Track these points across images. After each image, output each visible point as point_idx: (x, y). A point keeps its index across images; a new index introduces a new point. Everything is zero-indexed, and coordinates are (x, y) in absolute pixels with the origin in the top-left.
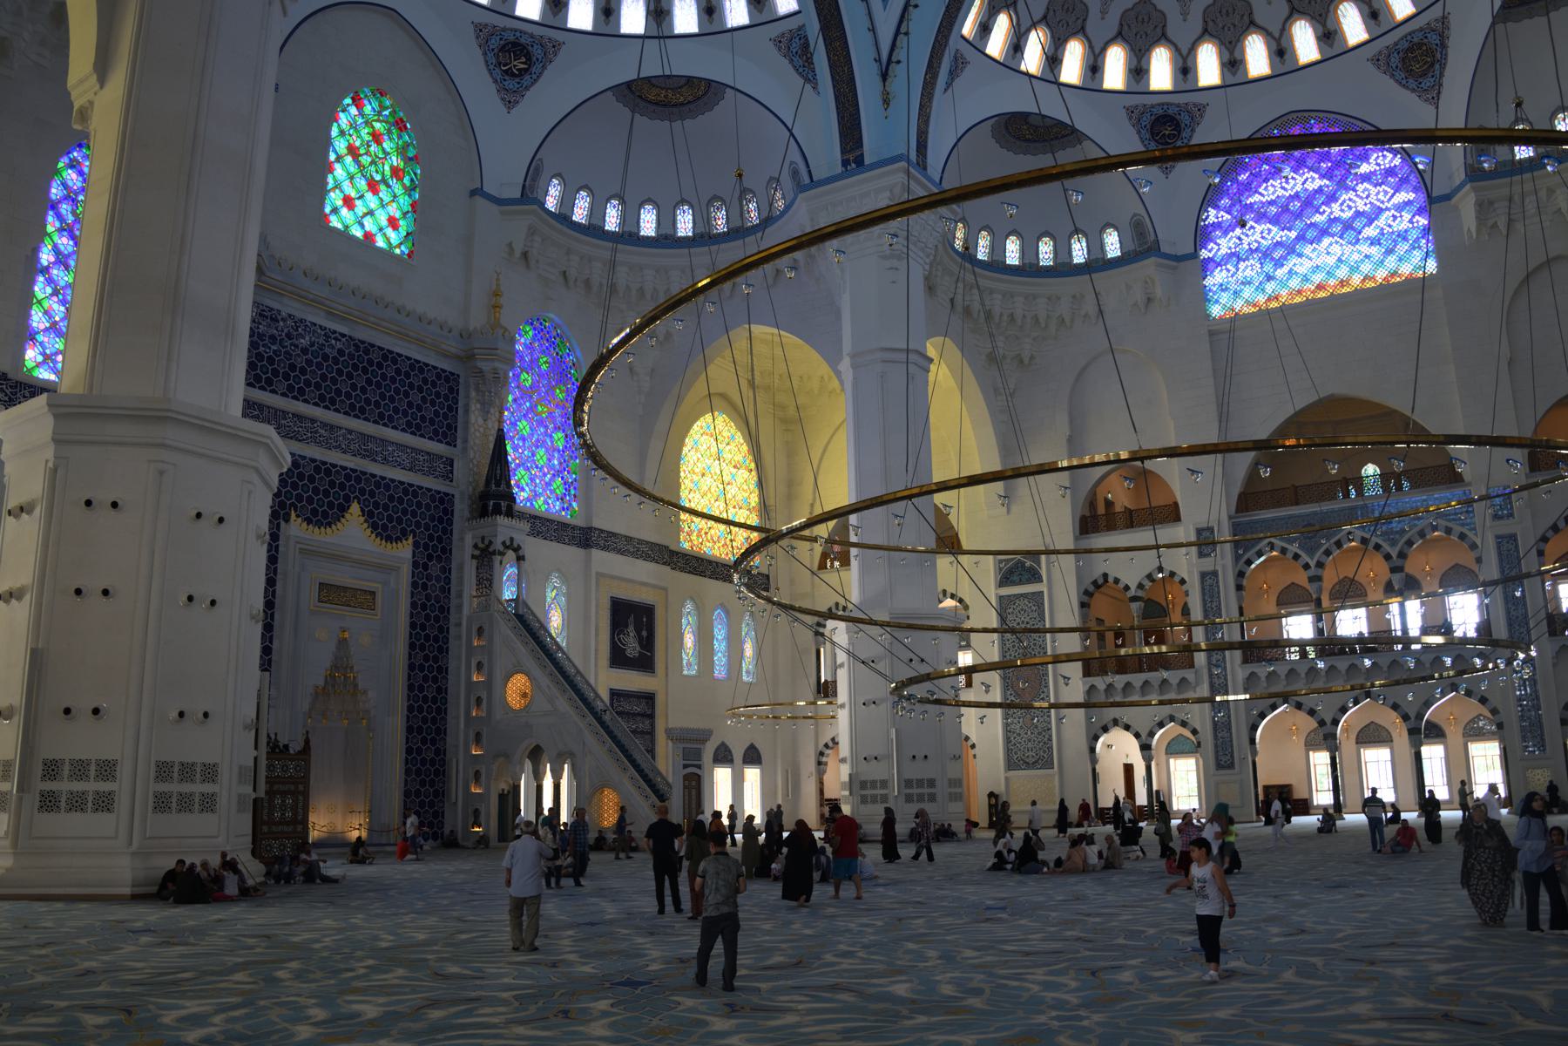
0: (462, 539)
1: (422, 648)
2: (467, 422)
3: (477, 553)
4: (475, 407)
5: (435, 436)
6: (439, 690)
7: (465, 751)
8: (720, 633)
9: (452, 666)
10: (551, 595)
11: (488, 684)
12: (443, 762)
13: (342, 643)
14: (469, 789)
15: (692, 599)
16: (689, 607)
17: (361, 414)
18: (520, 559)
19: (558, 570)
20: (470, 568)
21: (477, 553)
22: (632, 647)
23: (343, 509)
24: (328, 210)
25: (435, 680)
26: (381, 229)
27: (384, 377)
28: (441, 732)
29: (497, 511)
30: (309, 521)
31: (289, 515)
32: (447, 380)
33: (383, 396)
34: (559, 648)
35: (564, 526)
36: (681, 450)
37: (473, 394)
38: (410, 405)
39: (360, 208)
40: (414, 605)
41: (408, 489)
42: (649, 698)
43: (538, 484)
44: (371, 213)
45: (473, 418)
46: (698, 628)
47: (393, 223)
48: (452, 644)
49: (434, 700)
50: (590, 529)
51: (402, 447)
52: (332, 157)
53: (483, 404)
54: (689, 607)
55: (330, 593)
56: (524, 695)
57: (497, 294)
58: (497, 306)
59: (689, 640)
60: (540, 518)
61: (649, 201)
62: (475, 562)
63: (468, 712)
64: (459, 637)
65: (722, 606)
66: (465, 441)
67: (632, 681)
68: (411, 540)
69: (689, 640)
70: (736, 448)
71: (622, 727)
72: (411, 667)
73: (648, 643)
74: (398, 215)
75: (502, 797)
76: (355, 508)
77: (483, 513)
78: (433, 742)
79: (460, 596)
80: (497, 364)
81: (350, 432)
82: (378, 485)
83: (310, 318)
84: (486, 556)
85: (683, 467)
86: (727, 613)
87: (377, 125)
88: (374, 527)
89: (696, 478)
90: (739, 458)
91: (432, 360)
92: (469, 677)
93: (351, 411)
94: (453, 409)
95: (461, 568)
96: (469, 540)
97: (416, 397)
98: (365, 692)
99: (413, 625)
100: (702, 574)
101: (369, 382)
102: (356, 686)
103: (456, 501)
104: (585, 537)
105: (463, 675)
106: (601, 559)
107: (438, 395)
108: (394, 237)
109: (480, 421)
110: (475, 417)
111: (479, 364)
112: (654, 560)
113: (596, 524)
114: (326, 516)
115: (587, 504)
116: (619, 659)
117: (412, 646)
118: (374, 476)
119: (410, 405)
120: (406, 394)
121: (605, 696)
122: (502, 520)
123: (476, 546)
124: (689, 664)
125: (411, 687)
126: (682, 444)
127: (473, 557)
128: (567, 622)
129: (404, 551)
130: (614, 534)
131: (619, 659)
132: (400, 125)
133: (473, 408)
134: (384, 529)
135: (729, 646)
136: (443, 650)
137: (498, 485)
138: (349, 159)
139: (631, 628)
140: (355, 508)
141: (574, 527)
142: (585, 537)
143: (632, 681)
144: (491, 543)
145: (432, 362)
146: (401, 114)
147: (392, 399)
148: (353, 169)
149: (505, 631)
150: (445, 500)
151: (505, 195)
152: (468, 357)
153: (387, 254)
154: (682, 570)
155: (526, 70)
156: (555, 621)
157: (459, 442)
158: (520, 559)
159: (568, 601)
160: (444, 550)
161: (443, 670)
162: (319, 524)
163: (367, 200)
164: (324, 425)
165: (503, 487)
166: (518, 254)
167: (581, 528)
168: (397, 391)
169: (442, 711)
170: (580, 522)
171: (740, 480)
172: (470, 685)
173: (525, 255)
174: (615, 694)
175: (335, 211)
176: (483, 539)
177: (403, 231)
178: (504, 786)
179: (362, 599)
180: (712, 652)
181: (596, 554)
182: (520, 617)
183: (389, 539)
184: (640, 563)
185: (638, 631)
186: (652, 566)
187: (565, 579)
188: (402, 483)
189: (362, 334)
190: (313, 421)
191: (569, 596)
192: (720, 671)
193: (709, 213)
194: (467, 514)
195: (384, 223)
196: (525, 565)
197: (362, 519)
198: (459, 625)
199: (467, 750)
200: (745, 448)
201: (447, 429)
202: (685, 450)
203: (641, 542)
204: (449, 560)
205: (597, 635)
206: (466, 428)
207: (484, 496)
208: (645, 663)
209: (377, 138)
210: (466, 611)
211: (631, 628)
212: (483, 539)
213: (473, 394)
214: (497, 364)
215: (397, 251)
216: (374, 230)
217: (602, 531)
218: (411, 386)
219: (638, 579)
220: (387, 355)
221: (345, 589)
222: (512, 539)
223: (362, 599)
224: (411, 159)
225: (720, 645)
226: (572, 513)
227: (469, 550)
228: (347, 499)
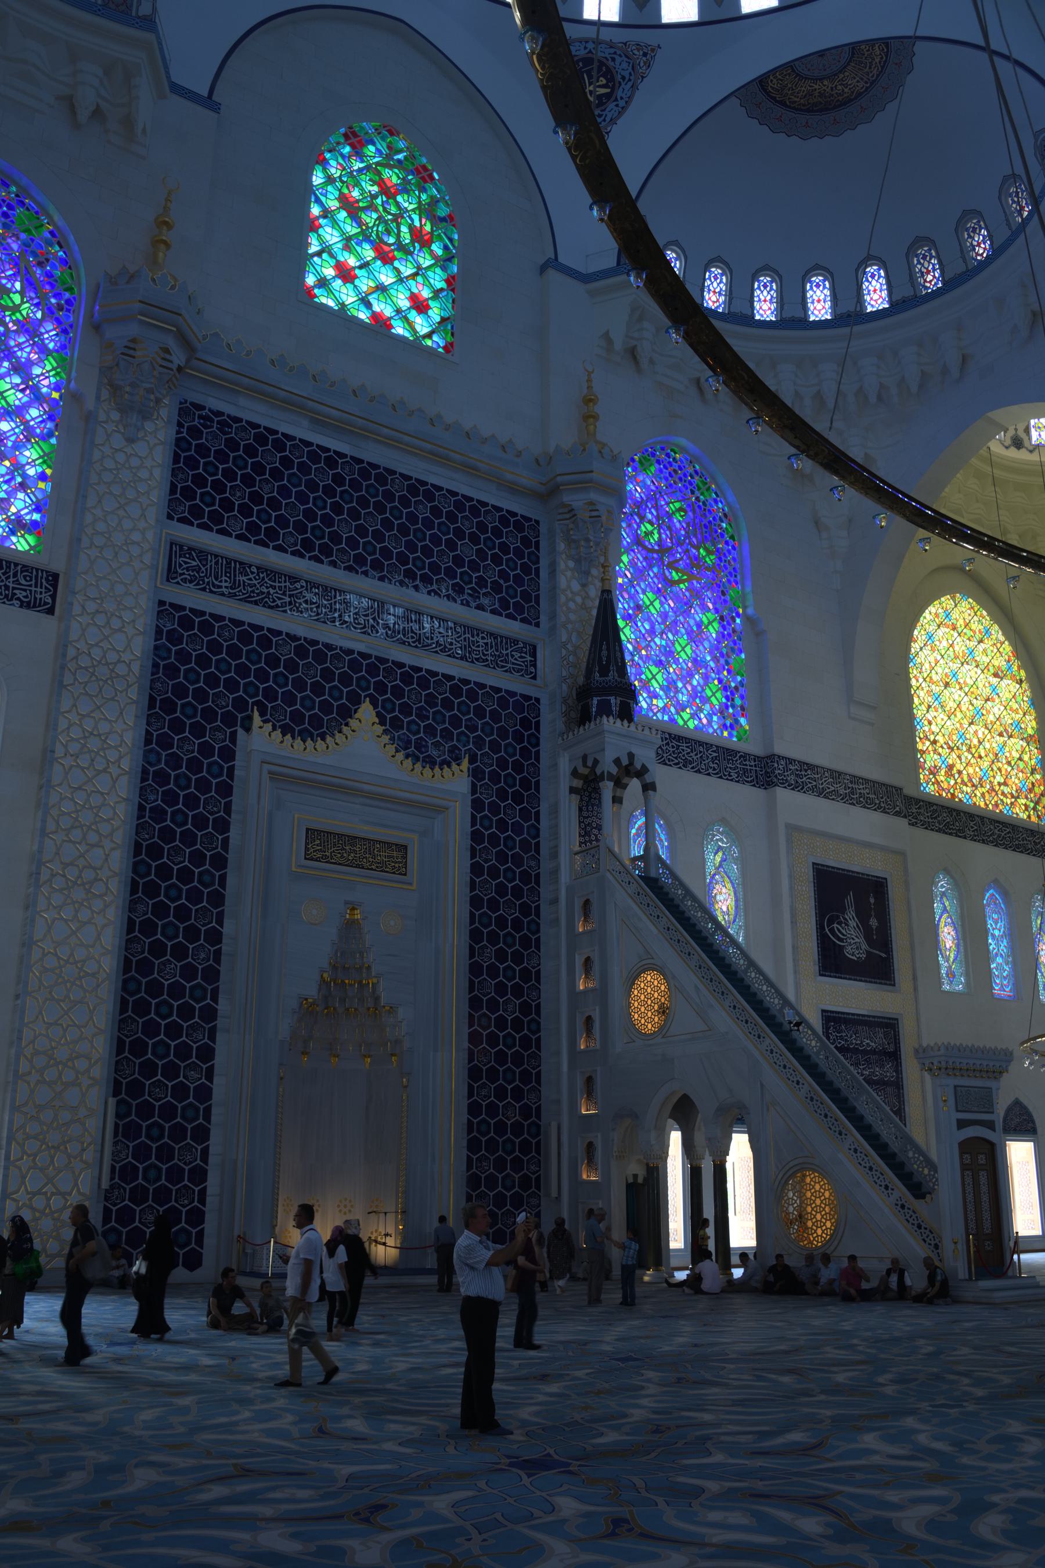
0: (555, 766)
1: (493, 938)
2: (554, 589)
3: (578, 783)
4: (565, 565)
5: (503, 609)
6: (525, 1008)
7: (570, 1107)
8: (996, 927)
9: (546, 967)
10: (714, 859)
11: (602, 994)
12: (537, 1130)
13: (350, 928)
14: (579, 1179)
15: (947, 872)
16: (943, 884)
18: (648, 787)
19: (723, 821)
20: (569, 808)
21: (578, 783)
22: (854, 943)
23: (346, 714)
24: (310, 280)
25: (518, 991)
26: (398, 311)
27: (412, 518)
28: (532, 1078)
29: (605, 709)
30: (285, 730)
31: (250, 718)
32: (519, 526)
33: (411, 547)
34: (734, 942)
35: (726, 753)
36: (908, 648)
37: (561, 546)
38: (458, 561)
39: (364, 283)
40: (476, 869)
41: (458, 686)
42: (889, 1026)
43: (677, 674)
44: (381, 288)
45: (562, 582)
46: (962, 917)
47: (420, 305)
48: (546, 932)
49: (517, 1025)
50: (772, 757)
52: (316, 210)
53: (578, 561)
54: (943, 884)
55: (325, 845)
56: (663, 1011)
57: (589, 400)
58: (589, 418)
59: (948, 936)
60: (687, 740)
61: (817, 268)
62: (575, 799)
63: (573, 1043)
64: (556, 921)
65: (997, 884)
66: (553, 616)
67: (857, 997)
68: (465, 764)
69: (948, 936)
70: (996, 649)
71: (847, 1073)
72: (475, 969)
73: (881, 940)
74: (426, 293)
75: (632, 1188)
76: (366, 712)
77: (585, 717)
78: (518, 1094)
79: (555, 855)
80: (592, 496)
82: (407, 678)
83: (284, 428)
84: (588, 787)
85: (914, 672)
86: (1005, 894)
87: (386, 173)
88: (404, 745)
89: (936, 689)
90: (999, 662)
91: (492, 497)
92: (572, 984)
94: (531, 569)
95: (555, 811)
96: (565, 766)
97: (467, 550)
98: (392, 1010)
99: (475, 902)
100: (960, 834)
101: (387, 524)
102: (377, 999)
103: (544, 708)
104: (764, 771)
105: (563, 981)
106: (792, 804)
107: (504, 548)
108: (422, 325)
109: (576, 586)
110: (567, 580)
111: (567, 498)
112: (878, 808)
113: (780, 749)
115: (763, 721)
116: (832, 961)
117: (475, 936)
118: (401, 665)
119: (458, 561)
120: (451, 545)
121: (815, 1021)
122: (611, 724)
123: (575, 773)
124: (951, 974)
125: (474, 1003)
126: (909, 639)
127: (573, 790)
128: (743, 903)
129: (455, 783)
130: (811, 767)
131: (832, 961)
132: (424, 176)
133: (562, 566)
135: (1012, 947)
136: (531, 943)
137: (604, 672)
138: (343, 214)
139: (850, 914)
140: (366, 712)
141: (745, 756)
142: (764, 771)
143: (857, 997)
144: (596, 762)
145: (492, 501)
146: (424, 160)
147: (427, 552)
148: (352, 229)
149: (623, 903)
150: (528, 706)
151: (593, 268)
152: (549, 493)
153: (414, 346)
154: (927, 826)
155: (608, 96)
156: (724, 901)
157: (543, 618)
158: (648, 787)
159: (744, 872)
160: (525, 784)
161: (532, 977)
162: (304, 735)
163: (372, 266)
164: (312, 585)
165: (613, 675)
166: (618, 345)
167: (756, 758)
168: (436, 540)
169: (531, 1044)
170: (754, 748)
171: (1006, 695)
172: (574, 994)
173: (632, 354)
174: (831, 1019)
175: (323, 283)
176: (585, 758)
177: (435, 313)
178: (635, 1169)
179: (388, 858)
180: (987, 957)
181: (783, 795)
182: (652, 883)
183: (430, 762)
185: (863, 917)
186: (877, 817)
187: (735, 834)
188: (449, 678)
189: (373, 453)
191: (744, 863)
192: (1002, 984)
193: (910, 268)
194: (560, 725)
195: (404, 304)
196: (656, 798)
197: (379, 729)
198: (555, 901)
199: (574, 1107)
200: (1007, 648)
201: (522, 598)
202: (915, 647)
204: (535, 799)
205: (794, 923)
206: (553, 598)
207: (584, 693)
208: (878, 969)
209: (387, 191)
210: (564, 878)
211: (850, 914)
212: (585, 758)
213: (561, 546)
214: (592, 496)
215: (429, 342)
216: (388, 312)
217: (791, 761)
218: (459, 533)
219: (859, 837)
220: (415, 486)
221: (353, 839)
222: (631, 756)
223: (388, 858)
224: (443, 219)
225: (998, 943)
226: (743, 735)
227: (565, 781)
228: (356, 700)
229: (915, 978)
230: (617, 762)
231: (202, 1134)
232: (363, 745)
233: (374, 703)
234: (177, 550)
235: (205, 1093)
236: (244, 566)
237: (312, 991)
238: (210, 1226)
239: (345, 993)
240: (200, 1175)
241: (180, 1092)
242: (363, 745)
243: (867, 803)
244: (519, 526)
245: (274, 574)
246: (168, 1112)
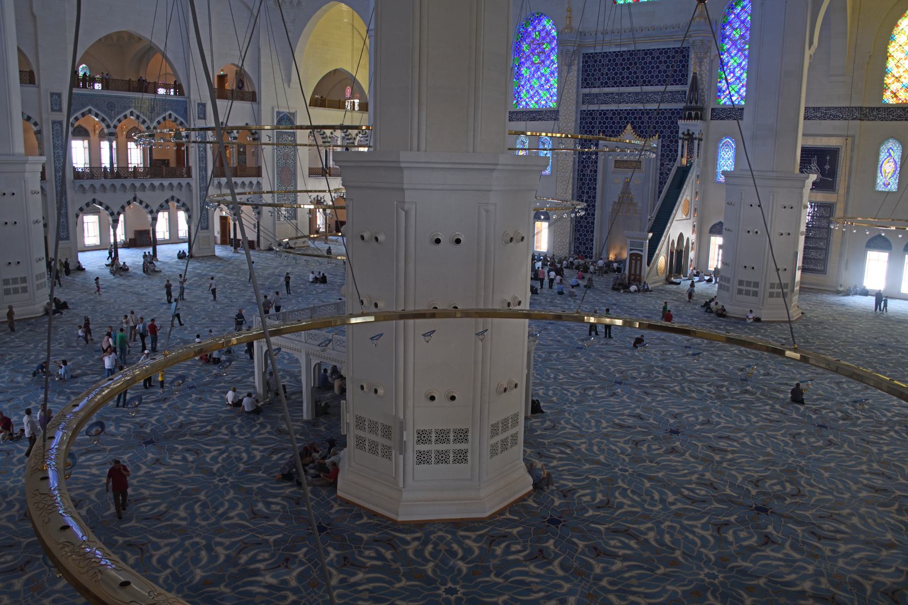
5: (675, 82)
17: (635, 84)
23: (625, 127)
51: (655, 93)
55: (619, 164)
76: (629, 127)
81: (629, 93)
93: (630, 84)
114: (617, 132)
129: (654, 143)
134: (641, 133)
140: (629, 127)
164: (617, 94)
184: (828, 122)
190: (612, 94)
203: (828, 109)
220: (647, 52)
229: (848, 187)
230: (683, 133)
231: (592, 232)
232: (629, 136)
233: (632, 123)
234: (585, 95)
235: (593, 223)
236: (600, 94)
237: (617, 200)
238: (594, 251)
239: (625, 198)
240: (592, 240)
241: (588, 223)
242: (629, 136)
243: (835, 118)
244: (682, 52)
245: (607, 94)
246: (586, 227)
